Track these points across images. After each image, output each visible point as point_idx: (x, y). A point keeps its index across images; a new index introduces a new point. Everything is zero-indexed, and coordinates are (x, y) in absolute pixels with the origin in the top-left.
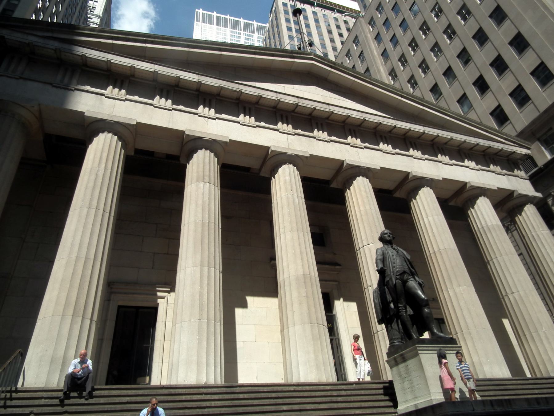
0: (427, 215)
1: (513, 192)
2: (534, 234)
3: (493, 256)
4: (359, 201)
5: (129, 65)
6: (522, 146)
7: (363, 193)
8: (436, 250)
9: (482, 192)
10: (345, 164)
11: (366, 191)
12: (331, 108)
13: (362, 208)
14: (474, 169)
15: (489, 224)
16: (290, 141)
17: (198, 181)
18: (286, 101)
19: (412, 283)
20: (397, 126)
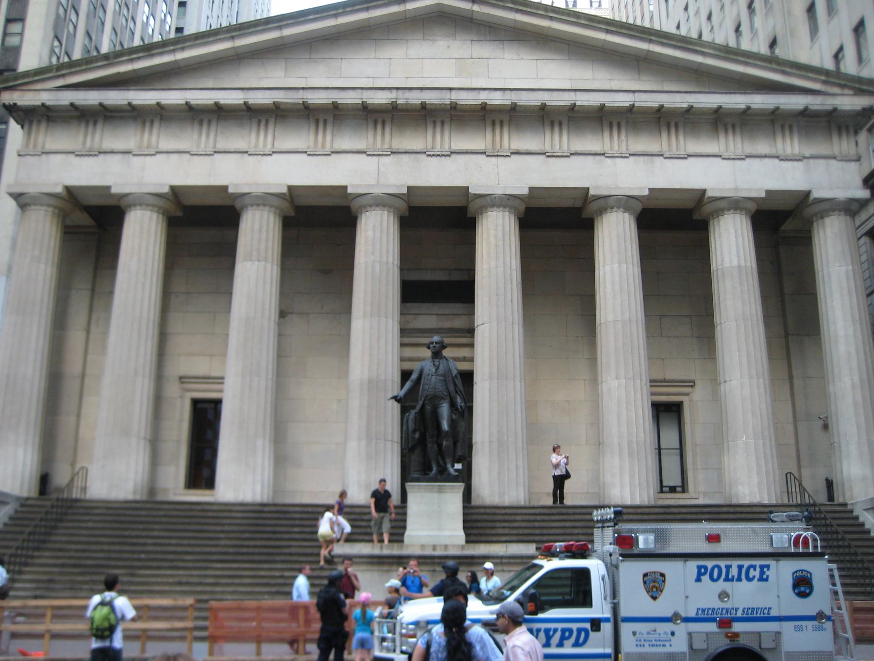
0: (604, 262)
1: (808, 193)
2: (825, 272)
3: (718, 322)
4: (484, 253)
5: (154, 102)
7: (492, 239)
9: (735, 204)
11: (496, 237)
12: (455, 96)
14: (733, 159)
15: (727, 264)
16: (381, 168)
17: (245, 260)
18: (376, 102)
19: (445, 409)
20: (578, 103)
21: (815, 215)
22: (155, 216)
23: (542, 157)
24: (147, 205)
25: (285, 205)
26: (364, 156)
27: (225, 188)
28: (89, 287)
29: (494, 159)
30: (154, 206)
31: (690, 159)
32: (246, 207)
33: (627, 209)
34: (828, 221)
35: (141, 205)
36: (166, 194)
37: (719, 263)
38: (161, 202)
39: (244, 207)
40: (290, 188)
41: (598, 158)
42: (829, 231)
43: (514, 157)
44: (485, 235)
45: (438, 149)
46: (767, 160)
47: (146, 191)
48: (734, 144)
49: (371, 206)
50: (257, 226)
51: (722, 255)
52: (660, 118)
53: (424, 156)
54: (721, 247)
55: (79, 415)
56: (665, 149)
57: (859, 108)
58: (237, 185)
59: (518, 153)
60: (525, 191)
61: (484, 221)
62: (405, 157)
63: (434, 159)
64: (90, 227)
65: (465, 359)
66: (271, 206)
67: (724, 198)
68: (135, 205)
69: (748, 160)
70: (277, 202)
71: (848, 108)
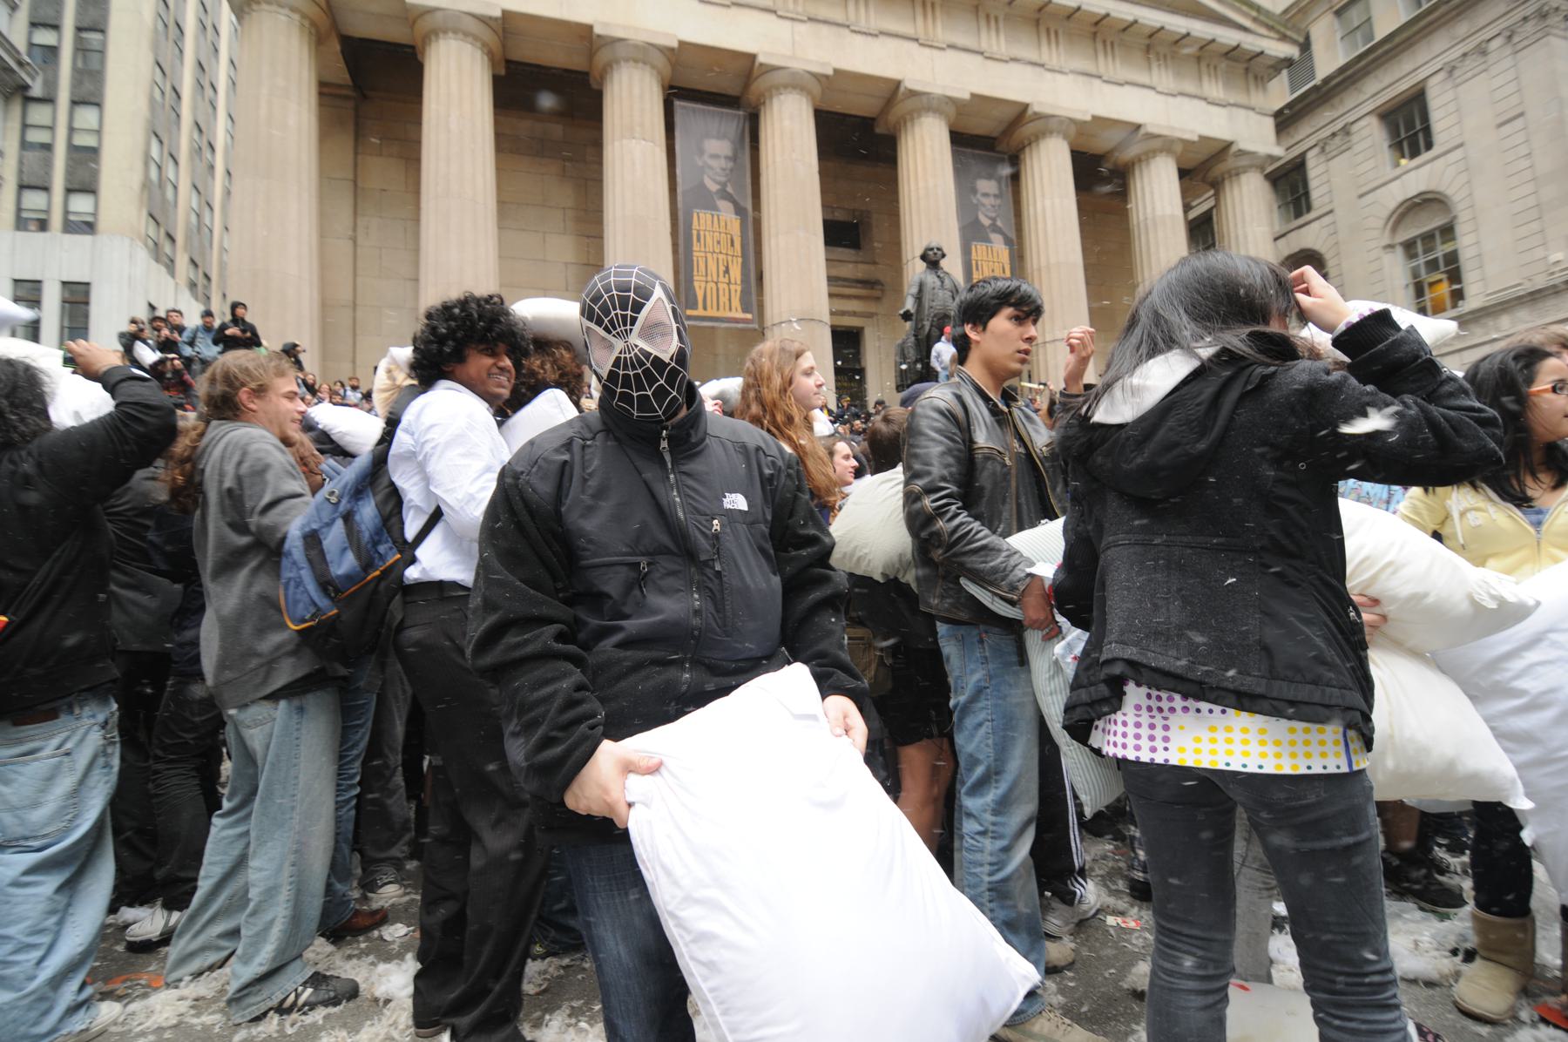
1: (1230, 144)
2: (1240, 232)
6: (1284, 38)
8: (1043, 263)
10: (902, 89)
13: (921, 184)
15: (1159, 212)
21: (1229, 172)
22: (478, 54)
23: (979, 58)
24: (466, 34)
25: (667, 71)
26: (773, 17)
27: (590, 28)
28: (351, 176)
29: (927, 51)
30: (476, 38)
31: (1127, 88)
32: (617, 62)
33: (1065, 137)
34: (1244, 178)
35: (455, 31)
36: (496, 19)
37: (1149, 210)
38: (488, 36)
39: (608, 67)
40: (682, 43)
41: (1038, 69)
42: (1245, 188)
43: (950, 52)
44: (918, 147)
45: (863, 25)
46: (1196, 102)
47: (465, 8)
48: (1163, 78)
49: (786, 87)
50: (636, 91)
51: (1153, 202)
52: (1095, 34)
53: (846, 31)
54: (1152, 193)
55: (354, 362)
56: (1102, 70)
57: (1282, 55)
58: (606, 25)
59: (952, 47)
60: (967, 96)
61: (917, 130)
62: (825, 29)
63: (859, 38)
64: (340, 86)
65: (843, 313)
66: (653, 67)
67: (1159, 136)
68: (445, 32)
69: (1179, 99)
70: (660, 61)
71: (1273, 53)
